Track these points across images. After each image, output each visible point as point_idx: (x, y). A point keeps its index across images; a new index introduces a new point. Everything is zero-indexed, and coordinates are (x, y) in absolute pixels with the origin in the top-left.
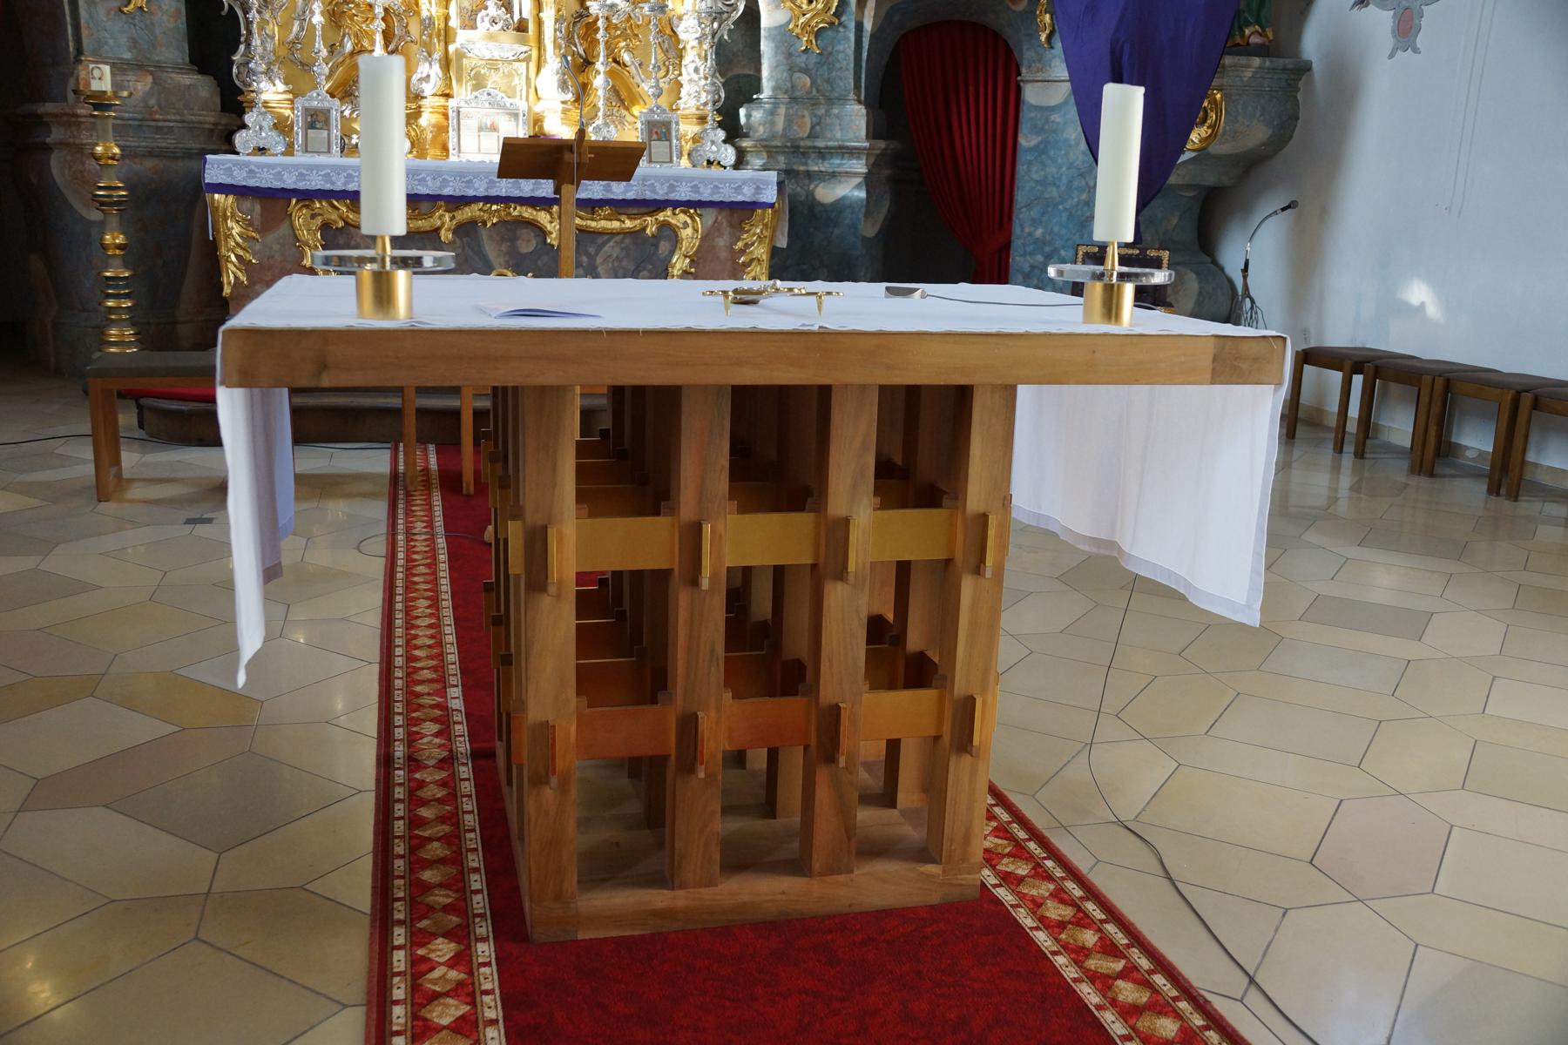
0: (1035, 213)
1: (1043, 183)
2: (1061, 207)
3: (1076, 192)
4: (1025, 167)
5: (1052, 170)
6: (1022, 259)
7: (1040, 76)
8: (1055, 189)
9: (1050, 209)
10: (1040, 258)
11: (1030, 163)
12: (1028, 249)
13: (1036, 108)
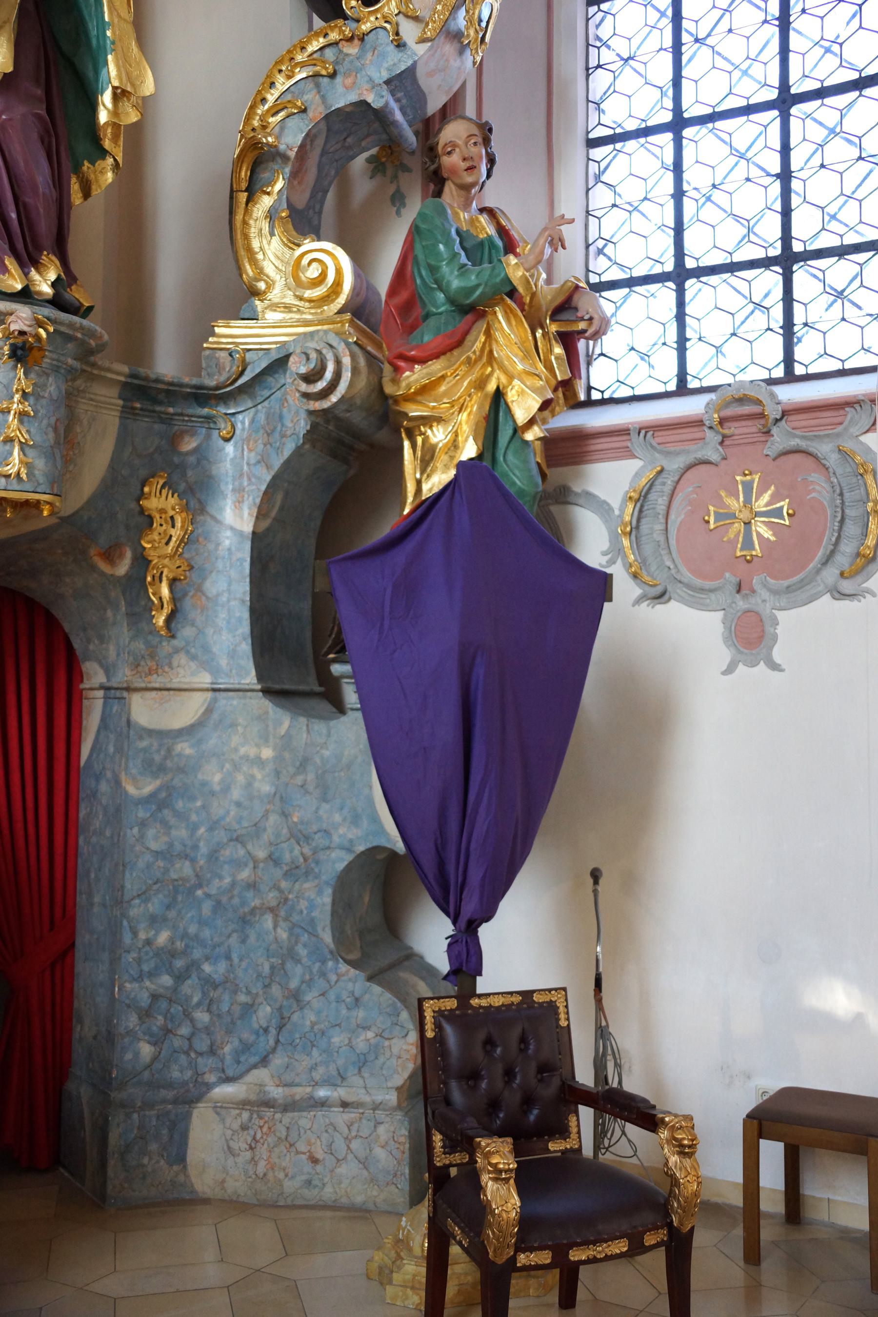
0: (155, 906)
1: (167, 855)
2: (199, 893)
3: (226, 867)
4: (136, 830)
5: (181, 833)
6: (136, 985)
7: (157, 681)
8: (187, 863)
9: (180, 898)
10: (166, 980)
11: (143, 824)
12: (146, 968)
13: (150, 732)
